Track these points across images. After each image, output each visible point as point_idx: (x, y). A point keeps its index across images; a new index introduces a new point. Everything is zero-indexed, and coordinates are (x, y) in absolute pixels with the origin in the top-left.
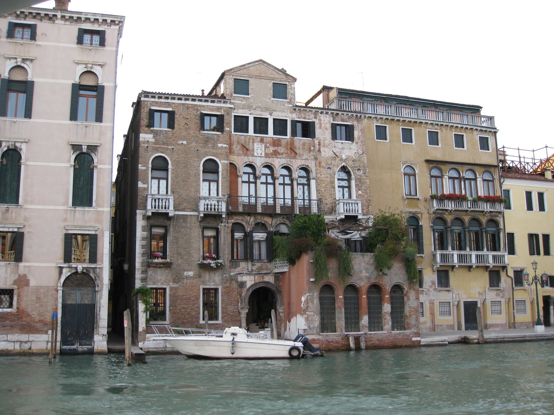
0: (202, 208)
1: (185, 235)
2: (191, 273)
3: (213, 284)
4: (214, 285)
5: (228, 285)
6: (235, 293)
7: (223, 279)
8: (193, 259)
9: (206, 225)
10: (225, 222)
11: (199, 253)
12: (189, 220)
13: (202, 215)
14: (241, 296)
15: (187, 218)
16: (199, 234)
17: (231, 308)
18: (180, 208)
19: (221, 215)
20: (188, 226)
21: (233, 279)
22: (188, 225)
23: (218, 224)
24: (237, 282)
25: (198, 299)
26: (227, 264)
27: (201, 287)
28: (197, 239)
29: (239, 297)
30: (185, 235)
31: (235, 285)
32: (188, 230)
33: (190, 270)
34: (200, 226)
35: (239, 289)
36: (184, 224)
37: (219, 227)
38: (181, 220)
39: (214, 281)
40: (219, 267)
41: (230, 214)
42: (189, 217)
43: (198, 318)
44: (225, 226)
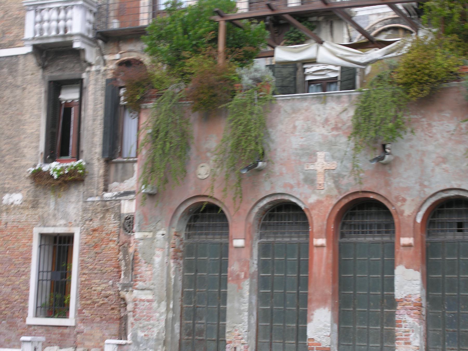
0: (29, 33)
1: (11, 104)
2: (16, 198)
3: (62, 222)
4: (65, 225)
5: (96, 224)
6: (112, 245)
7: (85, 210)
8: (24, 163)
9: (57, 73)
10: (98, 63)
11: (37, 147)
12: (21, 67)
13: (29, 49)
14: (126, 253)
15: (16, 64)
16: (39, 99)
17: (100, 286)
18: (5, 41)
19: (71, 43)
20: (19, 83)
21: (107, 208)
22: (20, 79)
23: (83, 70)
24: (119, 216)
25: (28, 260)
26: (98, 168)
27: (37, 231)
28: (36, 112)
29: (121, 256)
30: (11, 104)
31: (112, 224)
32: (18, 92)
33: (16, 190)
34: (43, 77)
35: (123, 237)
36: (10, 79)
37: (84, 76)
38: (5, 70)
39: (67, 215)
40: (73, 179)
41: (106, 38)
42: (22, 61)
43: (25, 309)
44: (98, 71)
